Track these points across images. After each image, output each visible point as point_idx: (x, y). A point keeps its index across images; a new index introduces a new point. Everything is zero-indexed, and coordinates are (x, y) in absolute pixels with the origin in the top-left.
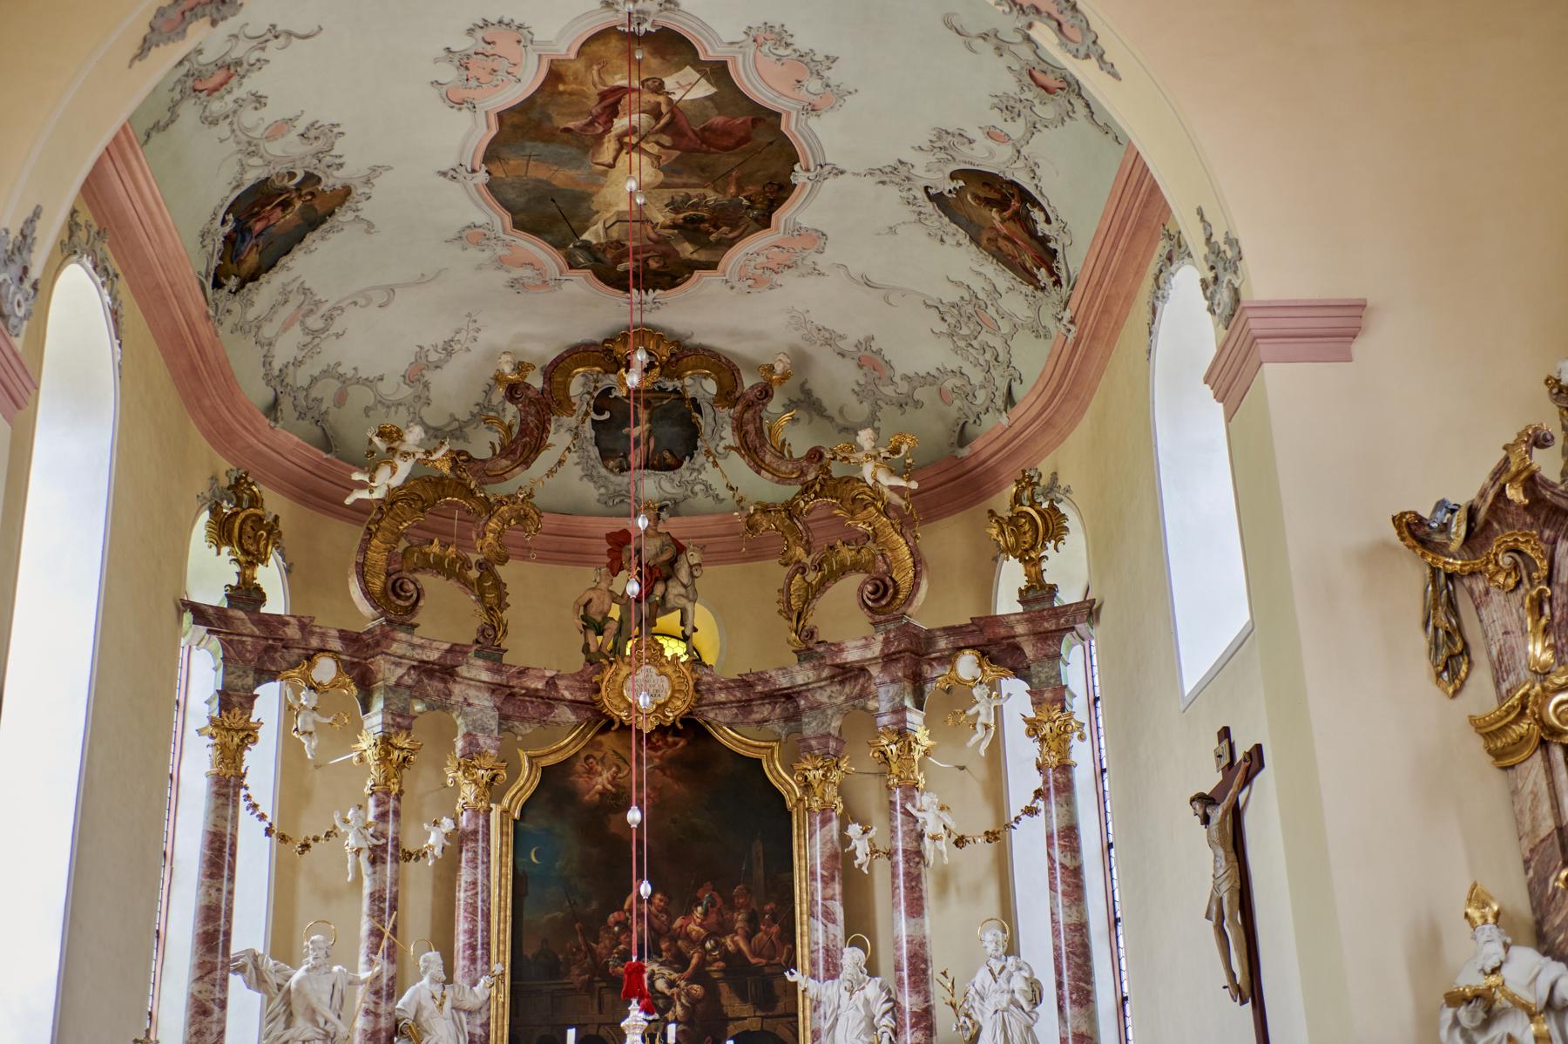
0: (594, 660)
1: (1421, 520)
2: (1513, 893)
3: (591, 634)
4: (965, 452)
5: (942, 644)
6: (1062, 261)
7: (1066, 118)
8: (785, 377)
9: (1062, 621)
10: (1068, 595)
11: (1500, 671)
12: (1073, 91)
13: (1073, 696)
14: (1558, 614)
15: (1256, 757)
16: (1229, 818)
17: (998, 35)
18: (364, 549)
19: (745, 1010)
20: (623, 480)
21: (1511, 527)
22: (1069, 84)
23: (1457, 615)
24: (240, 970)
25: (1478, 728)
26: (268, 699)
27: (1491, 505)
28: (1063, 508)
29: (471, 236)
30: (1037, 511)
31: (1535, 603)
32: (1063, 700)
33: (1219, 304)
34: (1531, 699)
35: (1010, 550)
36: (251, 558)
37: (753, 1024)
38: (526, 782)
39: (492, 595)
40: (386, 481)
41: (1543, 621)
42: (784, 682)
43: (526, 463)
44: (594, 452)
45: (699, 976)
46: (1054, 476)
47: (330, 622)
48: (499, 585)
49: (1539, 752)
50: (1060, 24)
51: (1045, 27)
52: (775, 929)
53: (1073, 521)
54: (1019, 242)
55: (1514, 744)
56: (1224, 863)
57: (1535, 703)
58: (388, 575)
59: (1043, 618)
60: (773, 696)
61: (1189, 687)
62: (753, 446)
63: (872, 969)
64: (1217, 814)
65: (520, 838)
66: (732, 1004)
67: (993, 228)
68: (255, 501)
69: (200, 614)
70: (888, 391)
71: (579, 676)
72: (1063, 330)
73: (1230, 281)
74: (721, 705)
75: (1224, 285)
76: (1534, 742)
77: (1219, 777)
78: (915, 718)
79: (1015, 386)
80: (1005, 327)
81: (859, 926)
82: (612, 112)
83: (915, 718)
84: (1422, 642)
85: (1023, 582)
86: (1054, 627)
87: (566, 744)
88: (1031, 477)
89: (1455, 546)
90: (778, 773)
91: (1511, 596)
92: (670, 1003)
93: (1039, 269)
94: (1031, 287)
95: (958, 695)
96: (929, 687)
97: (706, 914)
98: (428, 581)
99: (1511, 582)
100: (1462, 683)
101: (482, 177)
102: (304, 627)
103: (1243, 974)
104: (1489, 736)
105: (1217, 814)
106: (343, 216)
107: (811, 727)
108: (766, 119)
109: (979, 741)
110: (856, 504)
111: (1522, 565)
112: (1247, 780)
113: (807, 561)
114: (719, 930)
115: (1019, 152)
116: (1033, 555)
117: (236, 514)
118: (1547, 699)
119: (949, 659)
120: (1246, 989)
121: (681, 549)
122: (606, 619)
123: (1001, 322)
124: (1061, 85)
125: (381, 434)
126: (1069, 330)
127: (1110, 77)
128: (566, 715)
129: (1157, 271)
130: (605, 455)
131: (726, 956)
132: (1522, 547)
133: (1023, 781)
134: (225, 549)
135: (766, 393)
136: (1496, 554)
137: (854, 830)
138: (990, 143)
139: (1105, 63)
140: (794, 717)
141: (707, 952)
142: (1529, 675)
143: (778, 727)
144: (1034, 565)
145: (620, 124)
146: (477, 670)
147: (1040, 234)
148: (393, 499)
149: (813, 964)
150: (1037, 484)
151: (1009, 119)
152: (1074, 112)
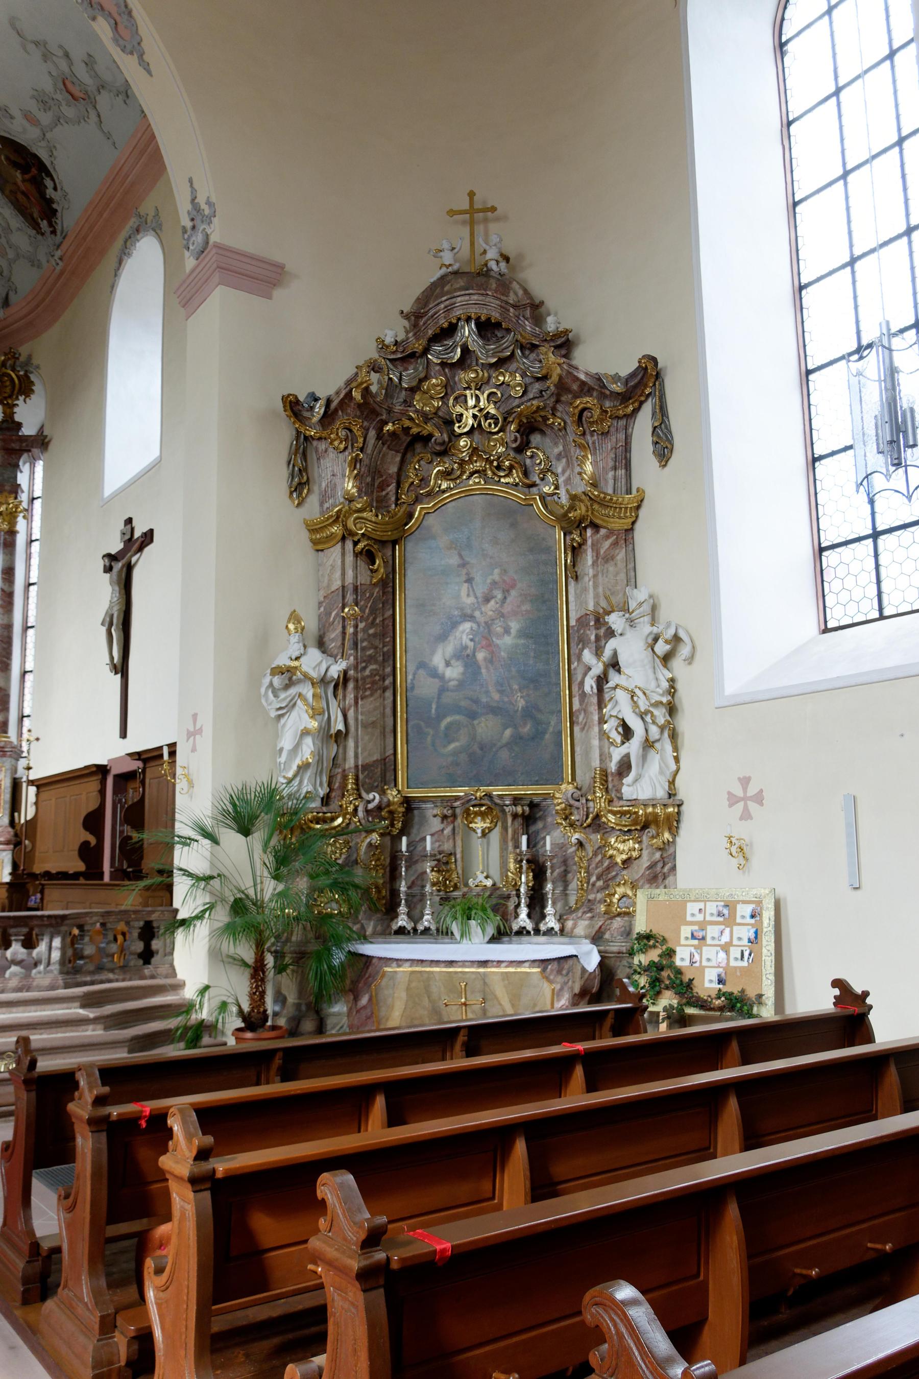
1: (297, 402)
2: (311, 623)
6: (60, 218)
7: (82, 121)
9: (24, 444)
12: (91, 103)
13: (23, 492)
14: (363, 470)
15: (148, 536)
16: (125, 569)
17: (47, 46)
21: (348, 415)
22: (89, 97)
23: (306, 461)
25: (307, 525)
27: (342, 400)
30: (16, 375)
31: (354, 461)
32: (16, 493)
33: (193, 244)
34: (343, 512)
41: (356, 472)
49: (340, 543)
50: (116, 23)
51: (105, 22)
54: (32, 199)
55: (327, 537)
56: (118, 595)
57: (345, 516)
59: (12, 441)
64: (118, 566)
67: (15, 184)
72: (54, 263)
73: (204, 229)
75: (200, 231)
76: (340, 537)
77: (121, 546)
79: (11, 294)
80: (11, 254)
86: (18, 448)
88: (15, 353)
89: (315, 419)
91: (340, 455)
93: (42, 220)
94: (34, 232)
99: (342, 446)
100: (303, 499)
103: (119, 659)
105: (118, 566)
111: (350, 438)
112: (141, 549)
115: (44, 135)
116: (10, 402)
118: (351, 514)
120: (119, 667)
123: (8, 250)
124: (82, 96)
126: (58, 264)
127: (146, 72)
129: (128, 236)
132: (352, 427)
136: (338, 429)
138: (25, 122)
139: (143, 61)
142: (342, 500)
144: (10, 408)
147: (48, 197)
150: (18, 358)
151: (42, 110)
152: (88, 118)
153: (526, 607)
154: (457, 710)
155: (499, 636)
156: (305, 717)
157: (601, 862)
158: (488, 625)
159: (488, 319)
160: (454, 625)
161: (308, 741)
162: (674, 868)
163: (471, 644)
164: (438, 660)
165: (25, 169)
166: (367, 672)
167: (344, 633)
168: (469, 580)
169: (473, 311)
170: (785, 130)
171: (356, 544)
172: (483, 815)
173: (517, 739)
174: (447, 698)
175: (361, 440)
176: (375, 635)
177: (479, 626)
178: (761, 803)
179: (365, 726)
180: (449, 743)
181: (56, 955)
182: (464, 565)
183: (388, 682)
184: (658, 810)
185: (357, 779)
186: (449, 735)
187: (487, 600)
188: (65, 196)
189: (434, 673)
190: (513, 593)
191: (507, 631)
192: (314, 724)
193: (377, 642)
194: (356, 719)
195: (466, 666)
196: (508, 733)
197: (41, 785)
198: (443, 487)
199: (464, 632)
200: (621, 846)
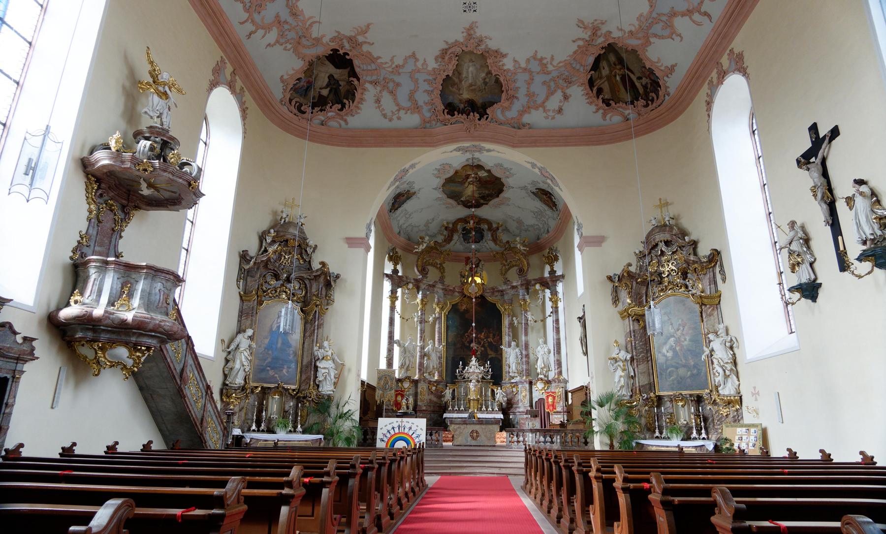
0: (463, 284)
4: (539, 241)
5: (533, 282)
8: (502, 225)
10: (559, 273)
11: (623, 304)
20: (469, 245)
24: (396, 343)
26: (399, 290)
28: (558, 255)
29: (438, 199)
35: (547, 263)
36: (396, 264)
38: (449, 307)
39: (442, 269)
40: (422, 247)
42: (501, 289)
43: (449, 243)
44: (462, 239)
45: (483, 346)
46: (557, 248)
47: (411, 277)
48: (443, 268)
53: (560, 258)
60: (498, 291)
61: (579, 295)
62: (495, 240)
63: (517, 346)
66: (490, 352)
68: (397, 252)
69: (387, 275)
70: (523, 228)
74: (488, 293)
78: (527, 297)
81: (515, 337)
82: (468, 178)
83: (527, 297)
84: (611, 298)
85: (549, 270)
90: (499, 306)
92: (477, 351)
95: (536, 292)
96: (530, 290)
98: (430, 268)
101: (441, 189)
102: (406, 278)
104: (621, 315)
106: (414, 197)
107: (506, 297)
108: (499, 179)
109: (540, 302)
110: (516, 253)
113: (506, 264)
114: (487, 337)
119: (534, 285)
121: (480, 261)
122: (465, 275)
125: (420, 238)
128: (457, 294)
130: (465, 240)
131: (488, 342)
133: (549, 309)
135: (498, 228)
137: (514, 318)
140: (503, 295)
143: (499, 297)
145: (469, 180)
146: (440, 286)
148: (423, 251)
153: (690, 332)
154: (673, 366)
155: (683, 342)
156: (621, 372)
157: (718, 415)
158: (679, 338)
159: (667, 240)
160: (669, 339)
161: (622, 379)
162: (742, 418)
163: (674, 345)
164: (664, 351)
165: (546, 195)
166: (641, 356)
167: (632, 345)
168: (672, 324)
169: (662, 239)
170: (758, 161)
172: (681, 400)
173: (692, 375)
175: (630, 286)
176: (642, 345)
178: (759, 395)
179: (641, 373)
181: (559, 441)
182: (669, 319)
184: (732, 398)
185: (640, 390)
186: (670, 374)
187: (678, 330)
188: (558, 201)
190: (686, 327)
191: (685, 340)
192: (623, 374)
194: (638, 371)
195: (674, 352)
196: (689, 373)
197: (573, 392)
198: (661, 294)
200: (725, 411)
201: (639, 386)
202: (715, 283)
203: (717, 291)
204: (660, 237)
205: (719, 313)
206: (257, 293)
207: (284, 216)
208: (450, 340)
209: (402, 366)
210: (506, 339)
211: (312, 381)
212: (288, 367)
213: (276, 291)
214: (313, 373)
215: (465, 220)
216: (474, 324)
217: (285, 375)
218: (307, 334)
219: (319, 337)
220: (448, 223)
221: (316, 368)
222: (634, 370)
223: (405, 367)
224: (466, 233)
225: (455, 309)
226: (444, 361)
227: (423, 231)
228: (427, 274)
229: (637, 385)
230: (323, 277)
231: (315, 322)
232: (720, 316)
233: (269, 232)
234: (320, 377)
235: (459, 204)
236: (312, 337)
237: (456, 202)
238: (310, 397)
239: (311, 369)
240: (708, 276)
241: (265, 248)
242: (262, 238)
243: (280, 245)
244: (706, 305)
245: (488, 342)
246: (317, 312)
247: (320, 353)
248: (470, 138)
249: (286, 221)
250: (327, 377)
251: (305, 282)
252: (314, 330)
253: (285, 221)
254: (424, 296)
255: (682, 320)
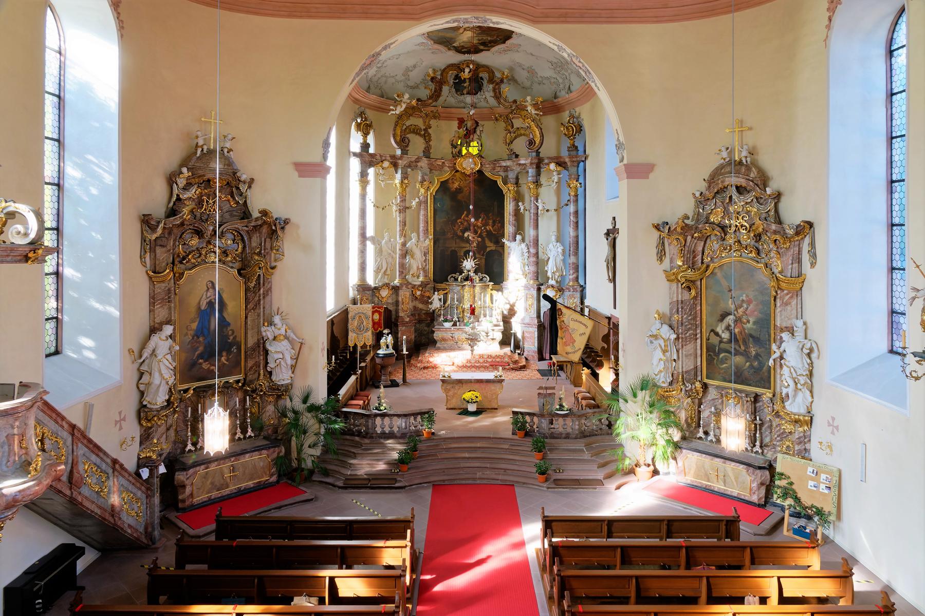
3: (453, 149)
18: (395, 130)
19: (492, 245)
26: (371, 171)
36: (366, 135)
37: (493, 248)
38: (434, 188)
39: (427, 137)
43: (436, 101)
45: (480, 236)
48: (429, 134)
52: (499, 225)
58: (401, 136)
65: (435, 199)
66: (488, 243)
71: (450, 160)
87: (446, 176)
97: (482, 221)
98: (410, 136)
114: (485, 225)
117: (361, 123)
131: (487, 231)
134: (359, 132)
141: (482, 230)
149: (509, 236)
161: (662, 362)
164: (720, 329)
166: (688, 335)
171: (682, 285)
174: (722, 345)
176: (691, 319)
177: (736, 317)
179: (686, 356)
180: (724, 364)
183: (699, 336)
185: (683, 376)
187: (741, 306)
189: (717, 334)
191: (748, 321)
193: (692, 322)
194: (682, 353)
196: (748, 364)
199: (730, 319)
201: (683, 372)
202: (800, 261)
203: (800, 275)
204: (733, 180)
205: (799, 302)
206: (173, 271)
207: (201, 142)
208: (438, 229)
209: (377, 271)
210: (509, 229)
211: (262, 368)
212: (227, 354)
213: (201, 254)
214: (262, 358)
215: (458, 67)
216: (471, 207)
217: (225, 364)
218: (250, 306)
219: (267, 307)
220: (434, 71)
221: (266, 352)
222: (678, 351)
223: (383, 271)
224: (458, 85)
225: (444, 185)
226: (431, 257)
227: (401, 81)
228: (407, 146)
229: (680, 371)
230: (265, 227)
231: (260, 290)
232: (799, 306)
233: (181, 173)
234: (271, 365)
235: (449, 49)
236: (257, 311)
237: (446, 49)
238: (261, 391)
239: (259, 353)
240: (792, 251)
241: (178, 195)
242: (171, 180)
243: (198, 187)
244: (783, 290)
245: (487, 231)
246: (262, 275)
247: (268, 332)
248: (472, 7)
249: (205, 151)
250: (282, 363)
251: (240, 234)
252: (259, 300)
253: (202, 150)
254: (405, 176)
255: (747, 296)
